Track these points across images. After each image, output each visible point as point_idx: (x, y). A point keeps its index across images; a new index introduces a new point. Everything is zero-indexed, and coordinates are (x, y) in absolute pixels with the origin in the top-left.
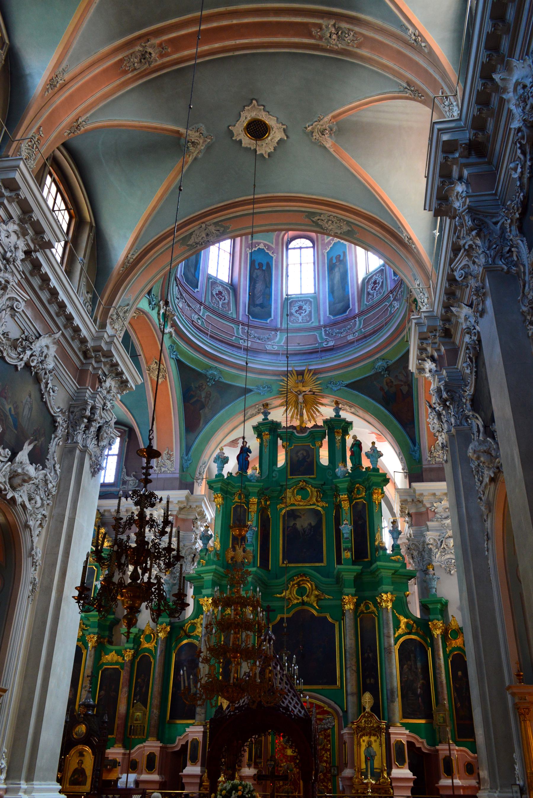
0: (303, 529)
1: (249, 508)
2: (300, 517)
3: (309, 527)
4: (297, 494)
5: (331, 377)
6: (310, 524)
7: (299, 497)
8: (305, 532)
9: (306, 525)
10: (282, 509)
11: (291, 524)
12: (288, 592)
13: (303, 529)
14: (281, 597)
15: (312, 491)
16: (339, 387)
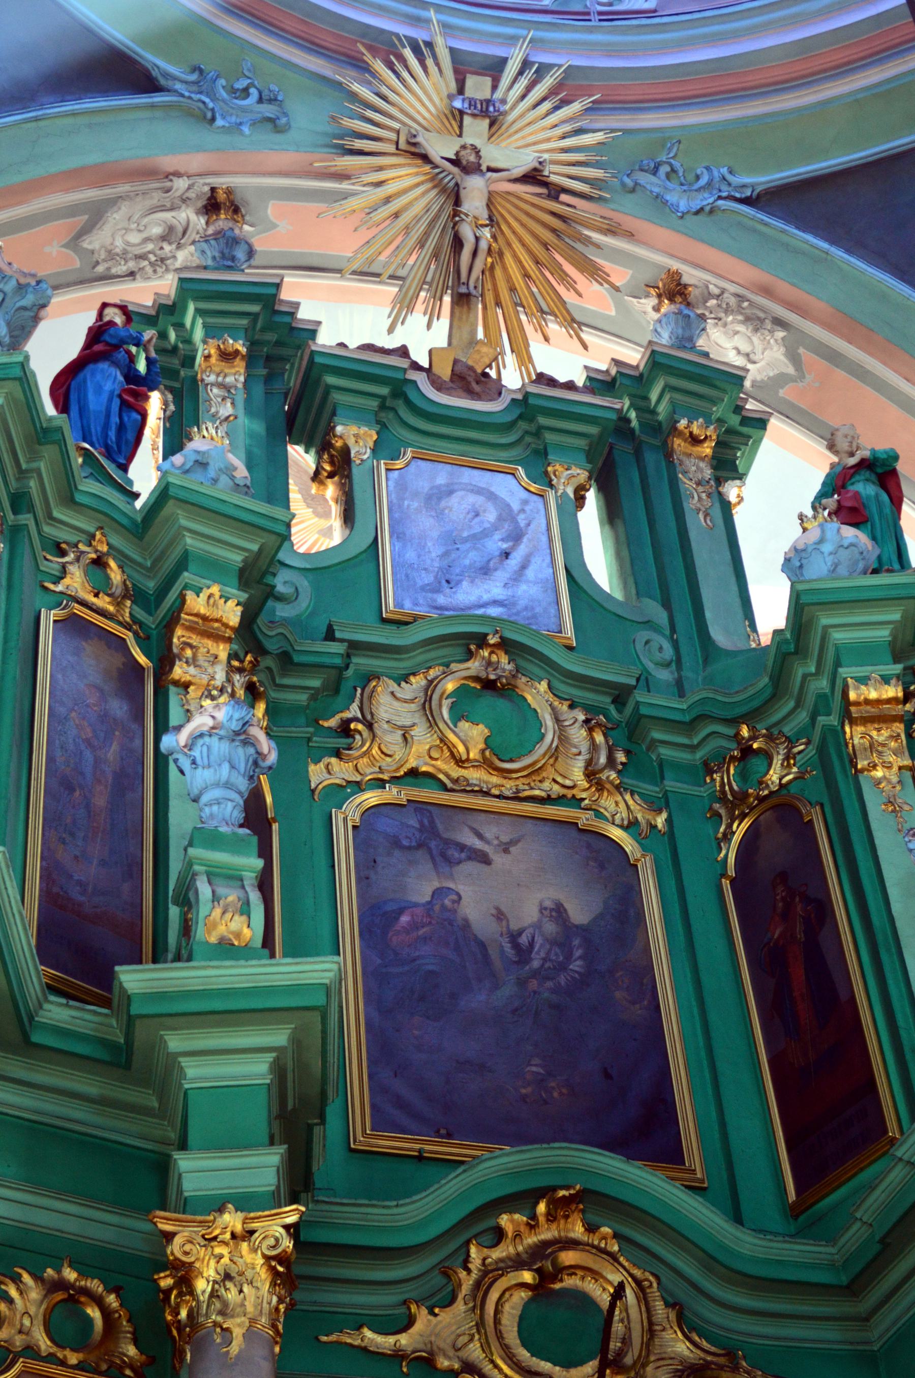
0: (513, 937)
1: (165, 660)
2: (485, 860)
3: (550, 928)
4: (458, 715)
5: (662, 139)
6: (558, 912)
7: (472, 736)
8: (523, 953)
9: (527, 913)
10: (341, 792)
11: (422, 886)
12: (454, 1319)
13: (513, 937)
14: (398, 1355)
15: (557, 720)
16: (706, 199)
